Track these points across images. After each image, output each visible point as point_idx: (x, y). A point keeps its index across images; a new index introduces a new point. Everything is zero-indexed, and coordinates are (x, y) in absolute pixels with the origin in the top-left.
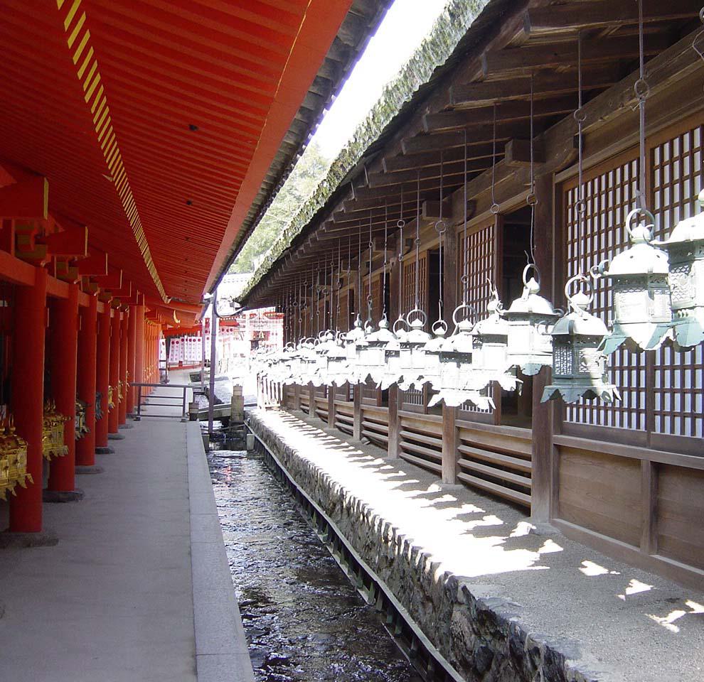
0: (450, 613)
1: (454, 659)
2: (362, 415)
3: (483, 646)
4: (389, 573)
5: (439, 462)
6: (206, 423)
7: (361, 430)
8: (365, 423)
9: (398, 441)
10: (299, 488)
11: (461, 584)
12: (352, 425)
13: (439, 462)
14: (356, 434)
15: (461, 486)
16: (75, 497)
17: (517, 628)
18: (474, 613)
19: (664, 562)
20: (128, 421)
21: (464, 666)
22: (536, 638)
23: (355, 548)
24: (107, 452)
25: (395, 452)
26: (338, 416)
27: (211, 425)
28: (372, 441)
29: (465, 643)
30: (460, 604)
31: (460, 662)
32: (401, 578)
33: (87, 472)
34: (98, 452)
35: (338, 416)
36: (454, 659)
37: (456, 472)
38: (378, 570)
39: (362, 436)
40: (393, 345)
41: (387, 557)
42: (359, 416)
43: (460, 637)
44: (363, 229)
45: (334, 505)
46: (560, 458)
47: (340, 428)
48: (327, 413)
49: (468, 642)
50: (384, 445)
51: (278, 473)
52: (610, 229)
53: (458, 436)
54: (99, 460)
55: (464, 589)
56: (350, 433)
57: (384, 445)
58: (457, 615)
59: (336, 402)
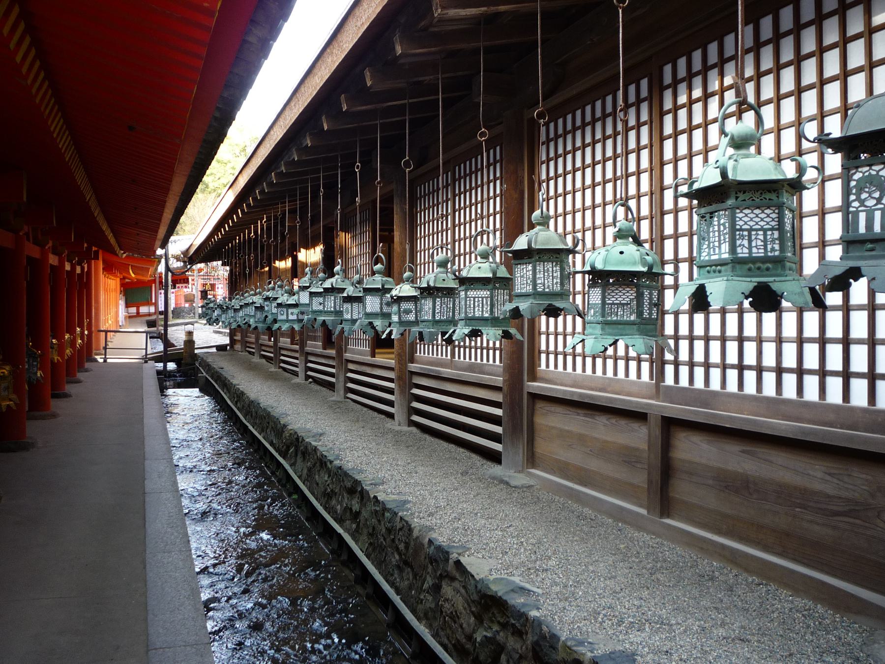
0: (436, 589)
1: (446, 641)
2: (306, 358)
3: (489, 635)
4: (354, 526)
5: (390, 403)
6: (161, 365)
7: (306, 372)
8: (310, 365)
9: (345, 383)
10: (251, 428)
11: (454, 556)
12: (297, 367)
13: (390, 403)
14: (302, 375)
15: (414, 429)
16: (25, 447)
17: (545, 628)
18: (475, 597)
19: (680, 529)
20: (87, 365)
21: (457, 650)
22: (575, 646)
23: (313, 494)
24: (66, 396)
25: (342, 392)
26: (282, 358)
27: (165, 366)
28: (316, 381)
29: (461, 626)
30: (453, 579)
31: (454, 645)
32: (370, 534)
33: (43, 418)
34: (55, 396)
35: (282, 358)
36: (446, 641)
37: (410, 415)
38: (340, 521)
39: (307, 377)
40: (350, 291)
41: (351, 509)
42: (303, 358)
43: (455, 617)
44: (313, 180)
45: (288, 448)
46: (534, 405)
47: (285, 369)
48: (272, 355)
49: (464, 626)
50: (331, 386)
51: (230, 417)
52: (609, 159)
53: (411, 379)
54: (56, 405)
55: (458, 563)
56: (296, 374)
57: (331, 386)
58: (447, 590)
59: (280, 344)
